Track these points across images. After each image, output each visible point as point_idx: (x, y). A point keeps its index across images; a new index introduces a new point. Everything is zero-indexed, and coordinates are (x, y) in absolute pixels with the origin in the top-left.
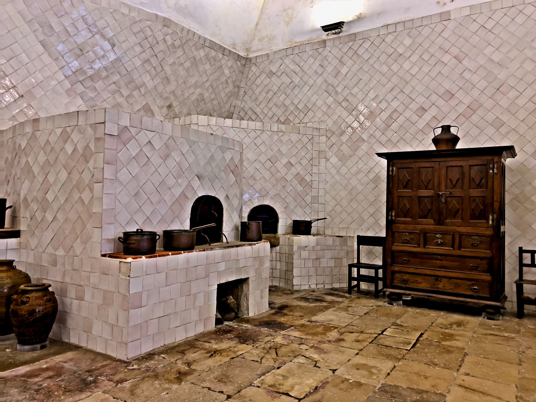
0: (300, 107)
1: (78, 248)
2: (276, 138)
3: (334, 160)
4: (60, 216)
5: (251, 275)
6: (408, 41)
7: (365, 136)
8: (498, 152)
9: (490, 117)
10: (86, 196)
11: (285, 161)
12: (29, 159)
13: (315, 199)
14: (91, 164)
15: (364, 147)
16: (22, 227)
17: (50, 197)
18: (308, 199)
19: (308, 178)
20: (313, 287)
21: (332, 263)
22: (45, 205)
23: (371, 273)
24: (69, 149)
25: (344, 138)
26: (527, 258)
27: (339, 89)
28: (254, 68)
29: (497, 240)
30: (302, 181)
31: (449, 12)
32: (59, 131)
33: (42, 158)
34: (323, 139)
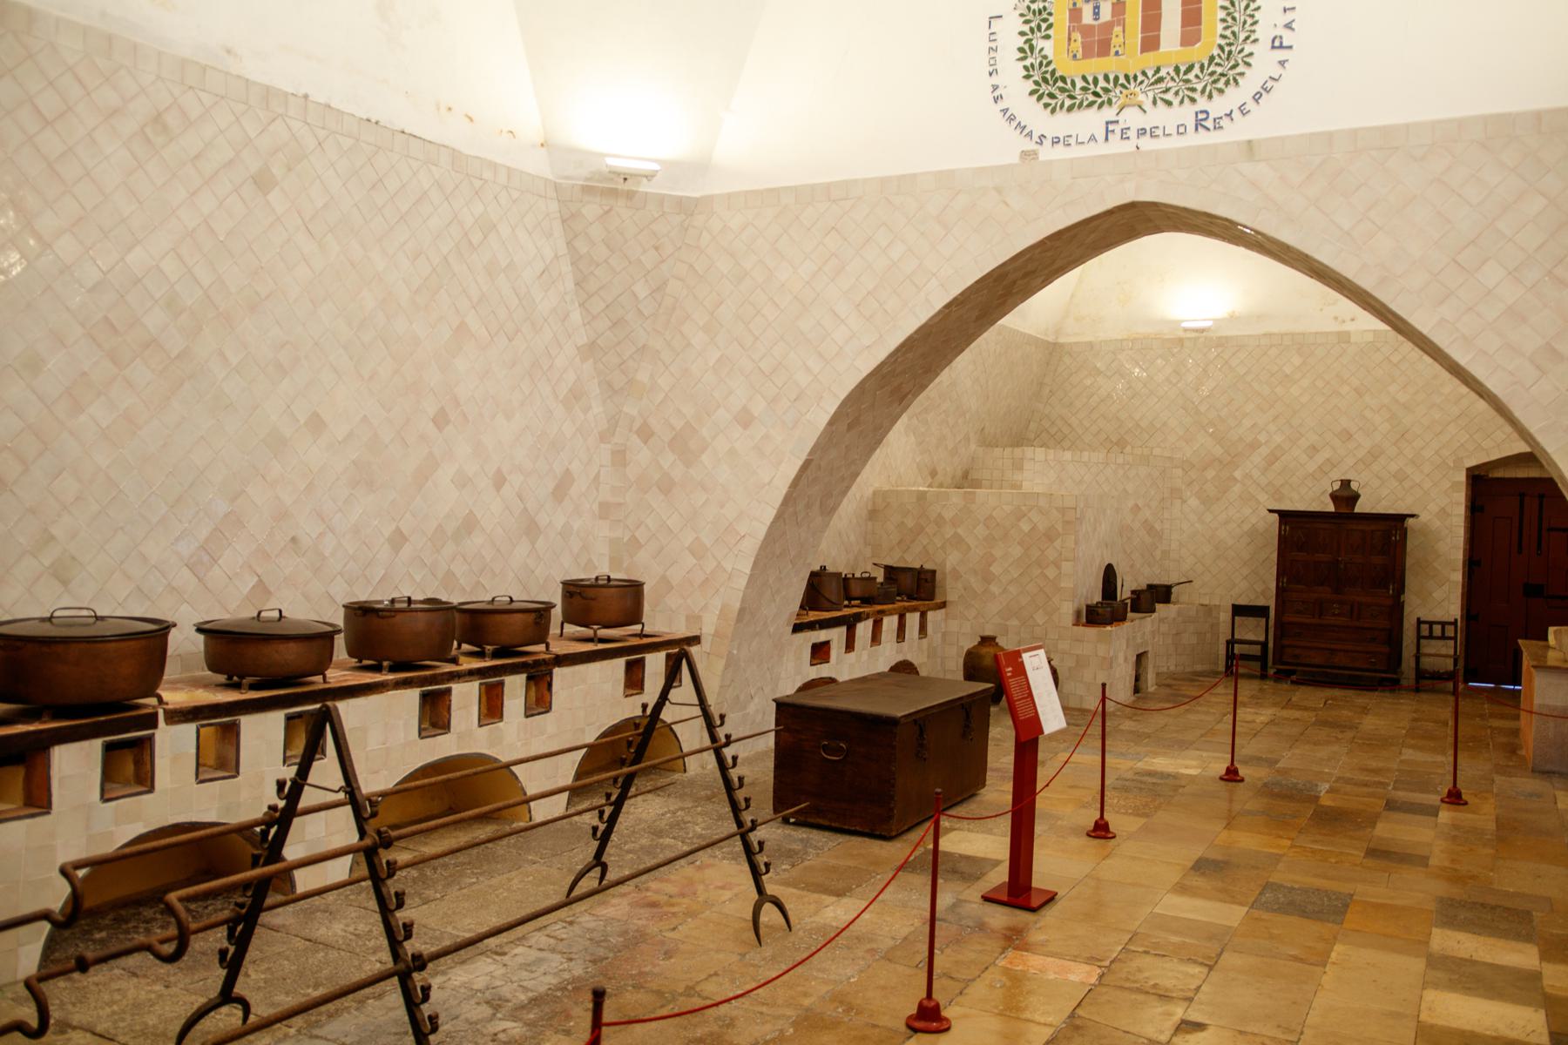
0: (1144, 424)
1: (1040, 618)
2: (1121, 472)
3: (1193, 502)
4: (1013, 589)
5: (1149, 648)
6: (1297, 360)
7: (1238, 474)
8: (1402, 518)
9: (1394, 467)
10: (1051, 572)
11: (1130, 504)
12: (960, 531)
13: (1166, 554)
14: (1058, 543)
15: (1237, 488)
16: (950, 598)
17: (995, 569)
18: (1158, 554)
19: (1158, 526)
20: (1172, 668)
21: (1194, 640)
22: (988, 578)
23: (1256, 650)
24: (1025, 526)
25: (1210, 474)
26: (1425, 629)
27: (1203, 409)
28: (1067, 360)
29: (1397, 609)
30: (1150, 529)
31: (1348, 333)
32: (1008, 508)
33: (981, 531)
34: (1179, 472)
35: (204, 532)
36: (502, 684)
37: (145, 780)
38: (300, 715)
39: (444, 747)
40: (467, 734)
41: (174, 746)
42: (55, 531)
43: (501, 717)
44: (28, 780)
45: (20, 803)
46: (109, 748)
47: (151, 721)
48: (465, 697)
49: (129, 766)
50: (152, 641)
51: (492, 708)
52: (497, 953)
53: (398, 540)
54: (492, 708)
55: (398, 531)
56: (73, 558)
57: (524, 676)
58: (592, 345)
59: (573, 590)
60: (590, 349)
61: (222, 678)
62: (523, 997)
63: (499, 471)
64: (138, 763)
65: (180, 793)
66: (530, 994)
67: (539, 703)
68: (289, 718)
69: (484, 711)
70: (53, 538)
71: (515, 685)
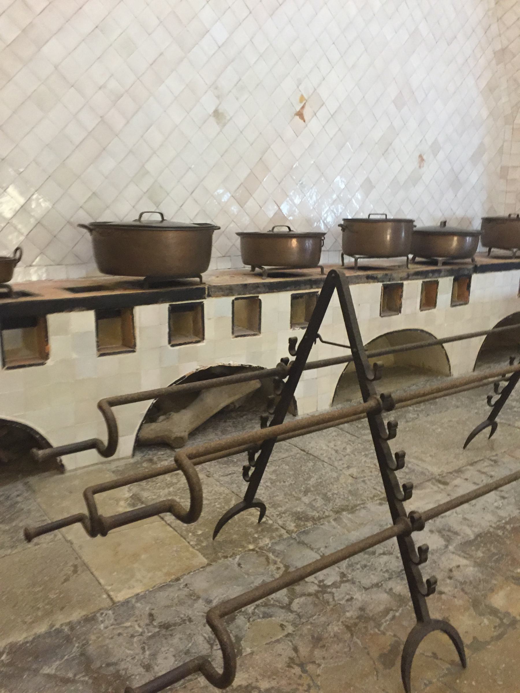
35: (243, 173)
36: (437, 283)
37: (199, 334)
38: (301, 296)
39: (397, 323)
40: (411, 315)
41: (217, 311)
42: (149, 167)
43: (434, 305)
44: (123, 328)
45: (120, 343)
46: (172, 310)
47: (201, 293)
48: (412, 290)
49: (186, 324)
50: (201, 236)
51: (429, 300)
52: (440, 482)
53: (368, 186)
54: (429, 300)
55: (368, 180)
56: (161, 187)
57: (452, 278)
58: (504, 50)
59: (487, 221)
60: (502, 55)
61: (248, 268)
62: (470, 533)
63: (436, 142)
64: (195, 321)
65: (220, 345)
66: (477, 530)
67: (461, 295)
68: (294, 297)
69: (424, 301)
70: (148, 172)
71: (446, 285)
